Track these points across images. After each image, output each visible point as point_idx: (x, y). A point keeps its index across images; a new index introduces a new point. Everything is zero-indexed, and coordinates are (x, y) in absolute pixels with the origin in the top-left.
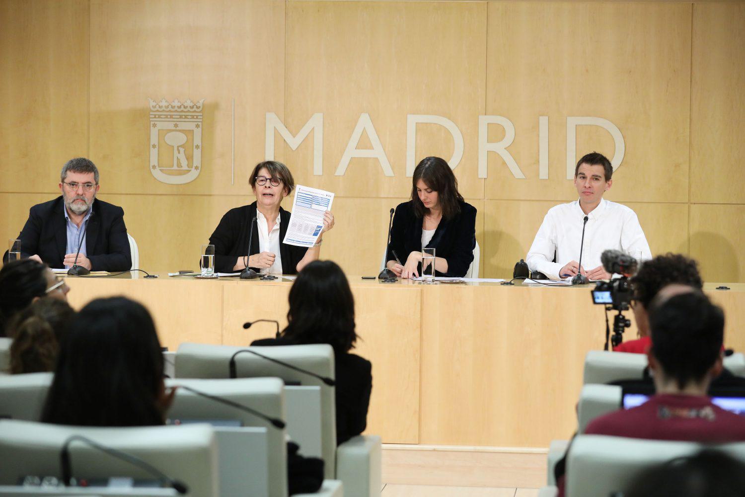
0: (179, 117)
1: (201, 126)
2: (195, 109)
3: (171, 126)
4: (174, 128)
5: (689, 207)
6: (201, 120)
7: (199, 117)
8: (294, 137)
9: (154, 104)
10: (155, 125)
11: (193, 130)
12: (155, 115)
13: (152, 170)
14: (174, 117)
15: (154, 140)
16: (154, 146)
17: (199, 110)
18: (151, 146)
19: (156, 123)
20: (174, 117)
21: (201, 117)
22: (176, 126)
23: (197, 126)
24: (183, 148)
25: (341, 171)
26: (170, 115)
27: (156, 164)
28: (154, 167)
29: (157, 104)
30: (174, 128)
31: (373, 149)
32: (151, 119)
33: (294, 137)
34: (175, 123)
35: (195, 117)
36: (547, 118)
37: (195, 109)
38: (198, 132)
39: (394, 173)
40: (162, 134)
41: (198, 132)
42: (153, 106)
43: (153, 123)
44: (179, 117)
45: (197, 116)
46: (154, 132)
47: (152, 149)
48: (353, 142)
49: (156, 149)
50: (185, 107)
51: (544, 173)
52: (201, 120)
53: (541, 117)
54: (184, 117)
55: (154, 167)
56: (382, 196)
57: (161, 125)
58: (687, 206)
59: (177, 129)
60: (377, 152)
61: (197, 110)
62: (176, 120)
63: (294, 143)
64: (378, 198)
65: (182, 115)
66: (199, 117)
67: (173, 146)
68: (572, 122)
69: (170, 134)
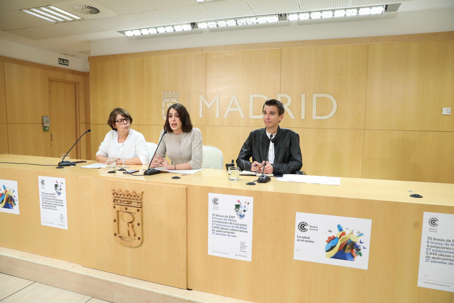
0: (171, 97)
3: (168, 101)
5: (364, 131)
6: (178, 98)
9: (163, 93)
10: (163, 101)
12: (164, 97)
13: (163, 116)
14: (170, 97)
15: (163, 106)
16: (163, 108)
17: (177, 95)
20: (170, 97)
21: (178, 97)
23: (177, 100)
25: (225, 116)
27: (164, 115)
28: (163, 115)
30: (170, 102)
31: (237, 108)
32: (162, 99)
33: (209, 104)
36: (305, 94)
39: (245, 117)
44: (171, 97)
46: (163, 103)
48: (230, 106)
49: (164, 109)
50: (173, 94)
51: (303, 117)
52: (178, 98)
53: (302, 94)
55: (163, 115)
57: (165, 101)
58: (363, 130)
59: (171, 102)
60: (239, 109)
61: (177, 95)
62: (170, 98)
63: (209, 106)
68: (315, 96)
69: (168, 104)
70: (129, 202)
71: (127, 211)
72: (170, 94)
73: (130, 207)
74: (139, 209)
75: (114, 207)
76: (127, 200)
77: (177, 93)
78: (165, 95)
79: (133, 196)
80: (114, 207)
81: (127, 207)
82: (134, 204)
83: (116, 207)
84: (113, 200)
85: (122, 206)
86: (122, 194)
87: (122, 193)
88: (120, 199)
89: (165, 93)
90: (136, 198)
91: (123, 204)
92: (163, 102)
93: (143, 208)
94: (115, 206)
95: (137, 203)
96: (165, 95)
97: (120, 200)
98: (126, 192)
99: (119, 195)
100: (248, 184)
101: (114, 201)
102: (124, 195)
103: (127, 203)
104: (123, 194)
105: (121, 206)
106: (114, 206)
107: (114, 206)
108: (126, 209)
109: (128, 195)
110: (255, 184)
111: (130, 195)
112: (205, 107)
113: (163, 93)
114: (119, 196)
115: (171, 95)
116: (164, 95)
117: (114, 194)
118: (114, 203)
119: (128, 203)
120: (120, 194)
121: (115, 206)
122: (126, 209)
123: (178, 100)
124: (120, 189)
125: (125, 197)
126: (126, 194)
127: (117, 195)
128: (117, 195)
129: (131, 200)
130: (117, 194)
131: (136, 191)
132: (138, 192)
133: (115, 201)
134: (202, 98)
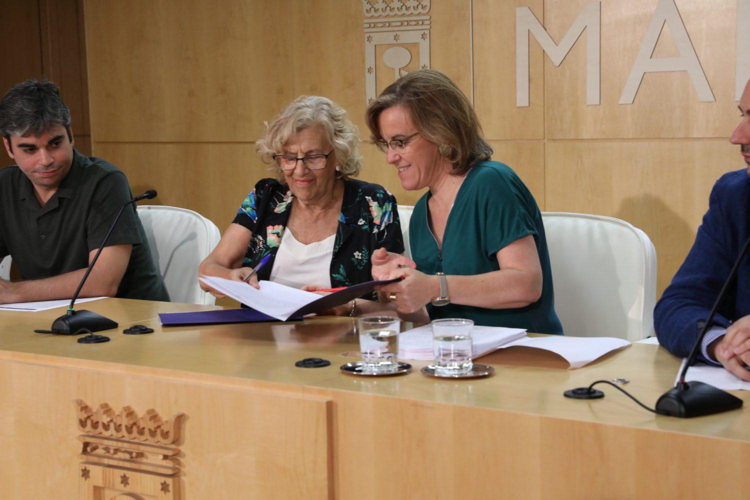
0: (399, 24)
1: (428, 36)
2: (420, 10)
3: (389, 38)
4: (395, 42)
6: (428, 27)
7: (426, 22)
8: (557, 45)
9: (369, 6)
10: (369, 39)
11: (419, 43)
12: (370, 24)
14: (393, 24)
15: (370, 62)
16: (370, 70)
18: (367, 70)
19: (372, 35)
20: (393, 24)
21: (428, 22)
22: (396, 37)
23: (423, 36)
24: (406, 71)
25: (626, 98)
26: (389, 22)
29: (372, 7)
30: (395, 42)
32: (366, 30)
34: (395, 34)
35: (421, 23)
37: (420, 10)
38: (424, 45)
40: (378, 50)
41: (424, 45)
42: (367, 10)
43: (367, 35)
45: (423, 21)
46: (369, 48)
47: (367, 74)
48: (646, 49)
49: (373, 74)
50: (407, 9)
52: (428, 27)
54: (406, 23)
56: (695, 136)
57: (378, 38)
59: (399, 42)
62: (396, 29)
63: (556, 54)
64: (687, 139)
65: (405, 21)
66: (426, 22)
67: (394, 69)
69: (388, 51)
70: (134, 455)
71: (128, 489)
72: (396, 11)
73: (139, 474)
74: (169, 481)
75: (85, 473)
76: (126, 445)
77: (424, 3)
78: (376, 15)
79: (146, 431)
80: (85, 473)
81: (129, 474)
82: (155, 459)
83: (91, 474)
84: (81, 446)
85: (111, 469)
86: (112, 425)
87: (109, 419)
88: (106, 442)
89: (376, 6)
90: (159, 437)
91: (115, 463)
92: (367, 43)
93: (183, 478)
94: (90, 467)
95: (161, 457)
96: (376, 15)
97: (107, 449)
98: (124, 414)
99: (100, 428)
100: (571, 394)
101: (85, 451)
102: (118, 428)
103: (127, 456)
104: (115, 424)
105: (108, 469)
106: (85, 469)
107: (85, 469)
108: (125, 480)
109: (132, 427)
110: (601, 396)
111: (138, 427)
112: (538, 56)
113: (369, 6)
114: (100, 428)
115: (400, 13)
116: (369, 15)
117: (83, 424)
118: (85, 457)
119: (131, 460)
120: (106, 427)
121: (90, 467)
122: (125, 480)
123: (427, 32)
124: (106, 405)
125: (120, 435)
126: (125, 422)
127: (95, 425)
128: (95, 425)
129: (142, 448)
130: (92, 421)
131: (159, 411)
132: (167, 416)
133: (89, 449)
134: (525, 20)
